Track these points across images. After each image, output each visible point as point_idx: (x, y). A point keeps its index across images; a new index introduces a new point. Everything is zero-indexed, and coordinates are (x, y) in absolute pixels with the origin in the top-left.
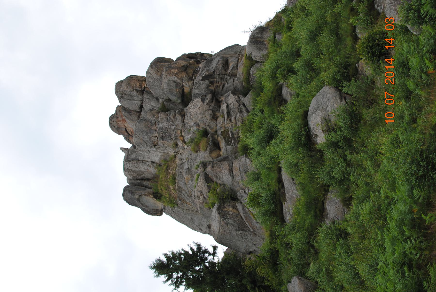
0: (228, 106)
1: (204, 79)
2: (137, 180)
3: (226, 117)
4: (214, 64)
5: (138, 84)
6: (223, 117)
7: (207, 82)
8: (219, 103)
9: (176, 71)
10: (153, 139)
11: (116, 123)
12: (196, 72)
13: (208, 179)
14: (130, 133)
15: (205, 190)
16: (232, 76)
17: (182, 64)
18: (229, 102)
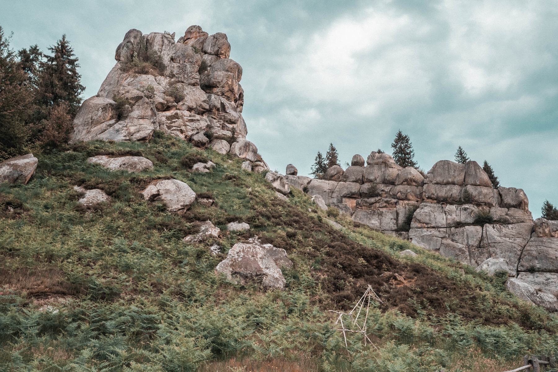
0: (198, 120)
1: (222, 104)
2: (147, 43)
3: (190, 118)
4: (233, 113)
5: (223, 52)
6: (190, 116)
7: (219, 106)
8: (202, 113)
9: (230, 83)
10: (178, 59)
11: (194, 31)
12: (228, 98)
13: (138, 98)
15: (129, 95)
16: (223, 126)
17: (235, 88)
18: (201, 122)
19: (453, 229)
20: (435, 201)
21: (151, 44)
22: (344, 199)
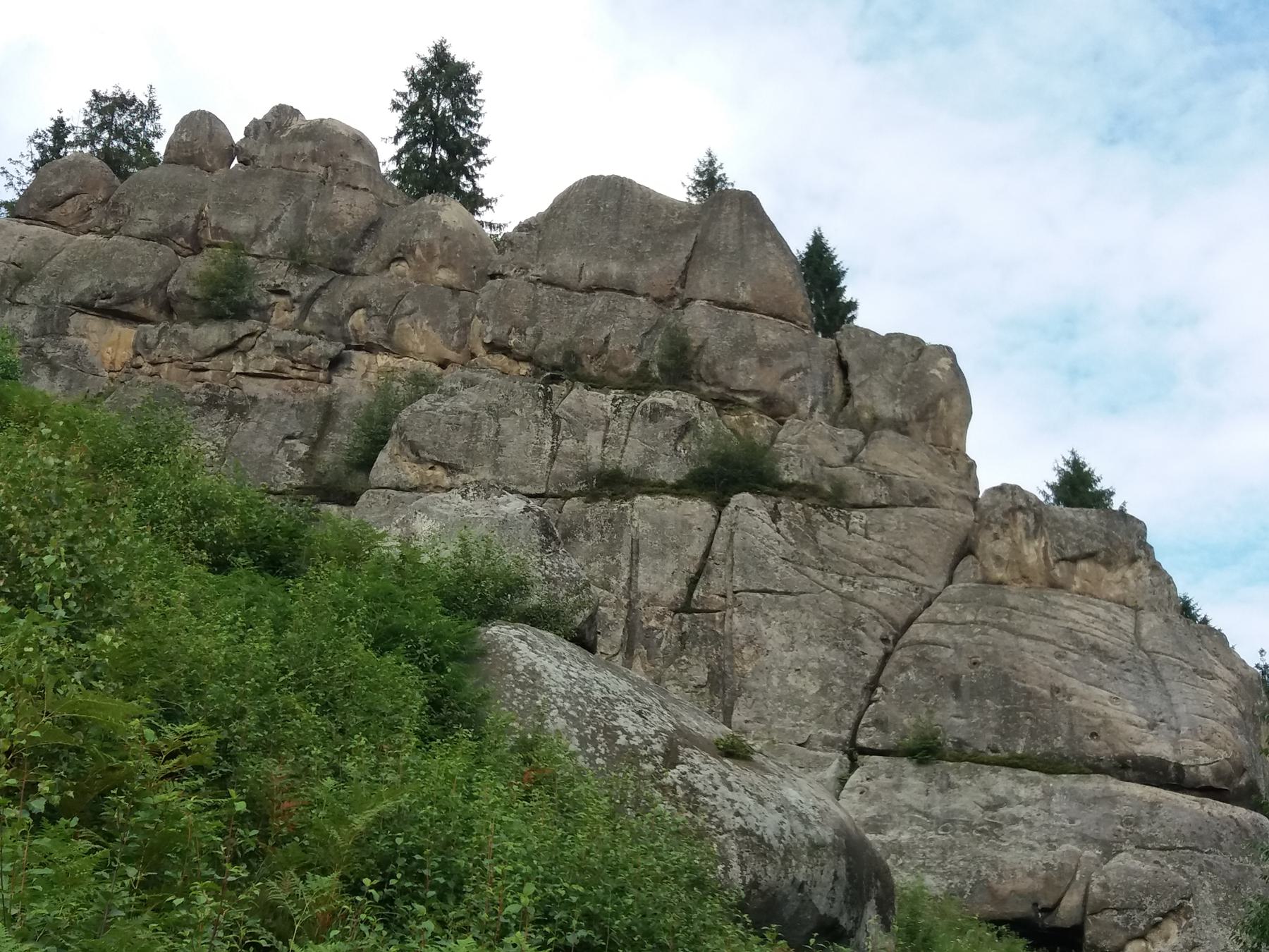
19: (574, 504)
20: (524, 368)
22: (77, 320)
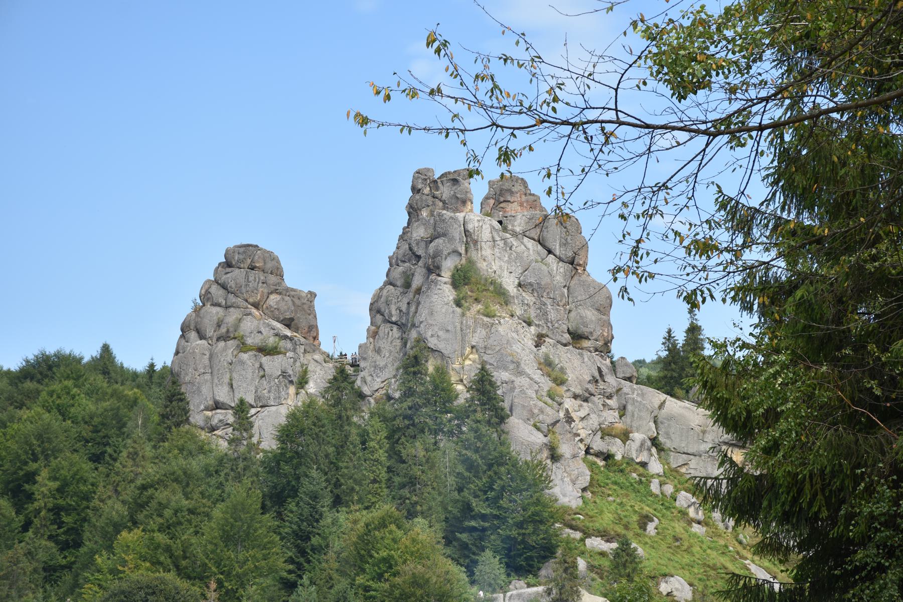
1: (599, 368)
8: (586, 400)
9: (606, 334)
14: (501, 205)
21: (476, 242)
